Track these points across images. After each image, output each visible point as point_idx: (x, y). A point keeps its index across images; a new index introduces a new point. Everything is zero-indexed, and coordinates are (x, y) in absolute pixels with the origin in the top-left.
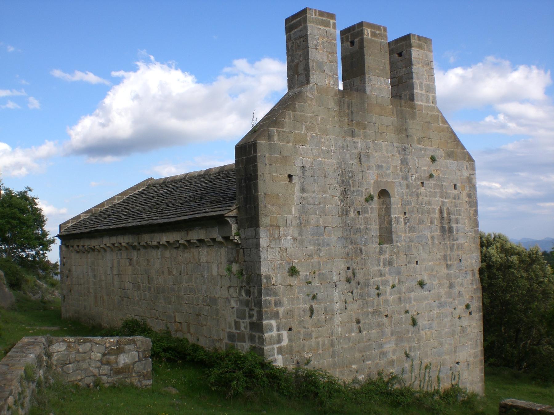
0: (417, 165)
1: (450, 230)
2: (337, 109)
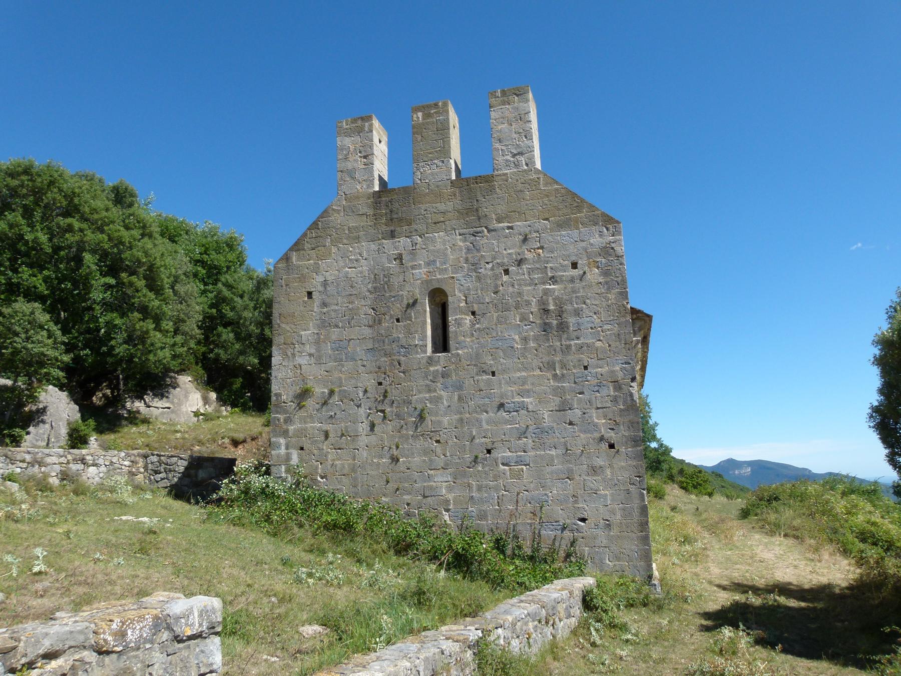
0: (497, 249)
1: (563, 327)
2: (370, 212)
